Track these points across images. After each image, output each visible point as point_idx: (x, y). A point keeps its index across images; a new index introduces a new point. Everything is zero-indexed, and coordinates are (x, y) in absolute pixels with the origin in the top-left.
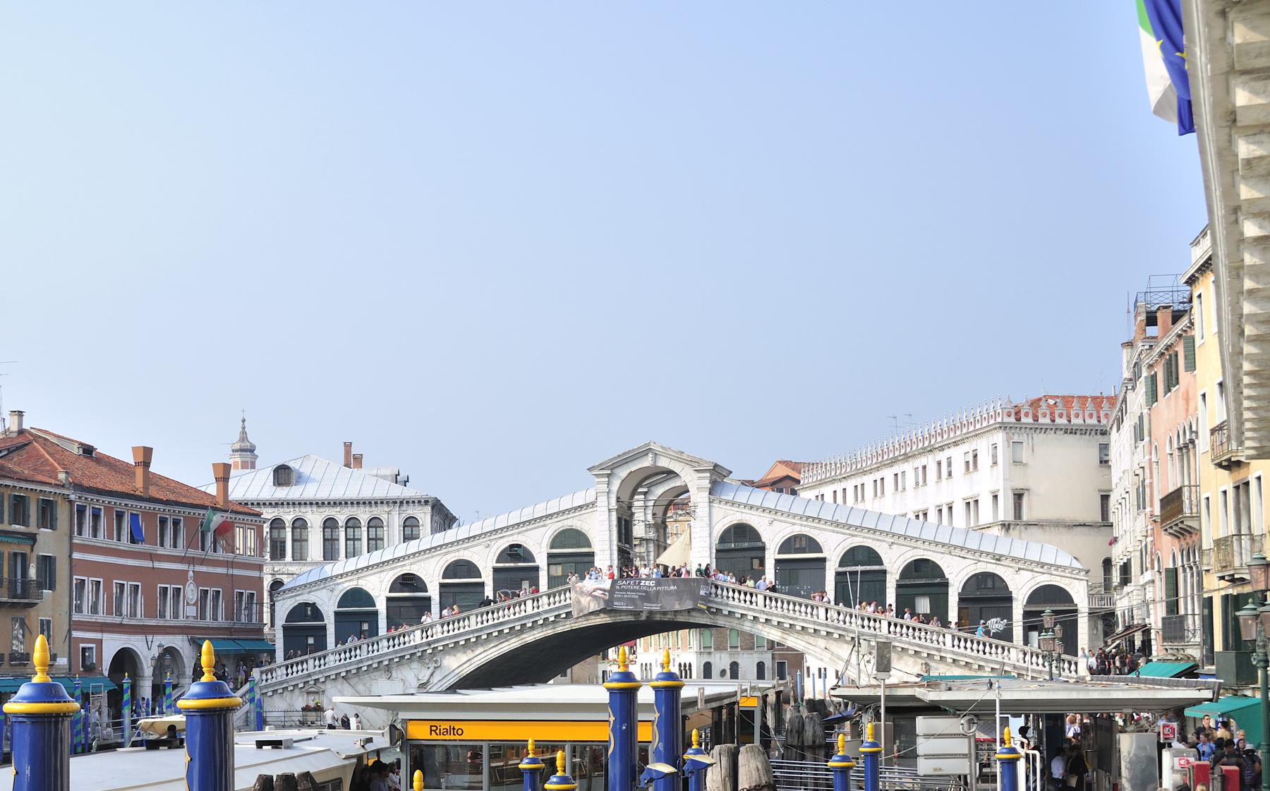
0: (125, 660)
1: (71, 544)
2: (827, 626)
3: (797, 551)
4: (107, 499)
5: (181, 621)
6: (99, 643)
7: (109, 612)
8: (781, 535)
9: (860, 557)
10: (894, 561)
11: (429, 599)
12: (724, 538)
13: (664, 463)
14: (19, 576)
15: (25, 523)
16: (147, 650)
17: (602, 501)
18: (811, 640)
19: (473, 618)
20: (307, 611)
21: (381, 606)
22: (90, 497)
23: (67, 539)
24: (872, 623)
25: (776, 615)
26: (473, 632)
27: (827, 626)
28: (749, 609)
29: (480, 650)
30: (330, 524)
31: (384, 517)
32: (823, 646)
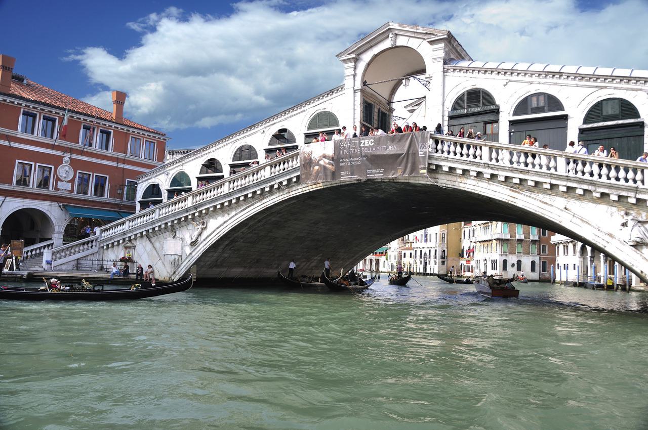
2: (568, 179)
3: (535, 111)
5: (51, 190)
8: (517, 96)
9: (610, 112)
12: (457, 104)
13: (401, 41)
17: (348, 83)
18: (547, 198)
19: (227, 184)
20: (154, 190)
24: (631, 175)
25: (503, 169)
27: (568, 179)
28: (471, 163)
29: (234, 213)
32: (562, 208)
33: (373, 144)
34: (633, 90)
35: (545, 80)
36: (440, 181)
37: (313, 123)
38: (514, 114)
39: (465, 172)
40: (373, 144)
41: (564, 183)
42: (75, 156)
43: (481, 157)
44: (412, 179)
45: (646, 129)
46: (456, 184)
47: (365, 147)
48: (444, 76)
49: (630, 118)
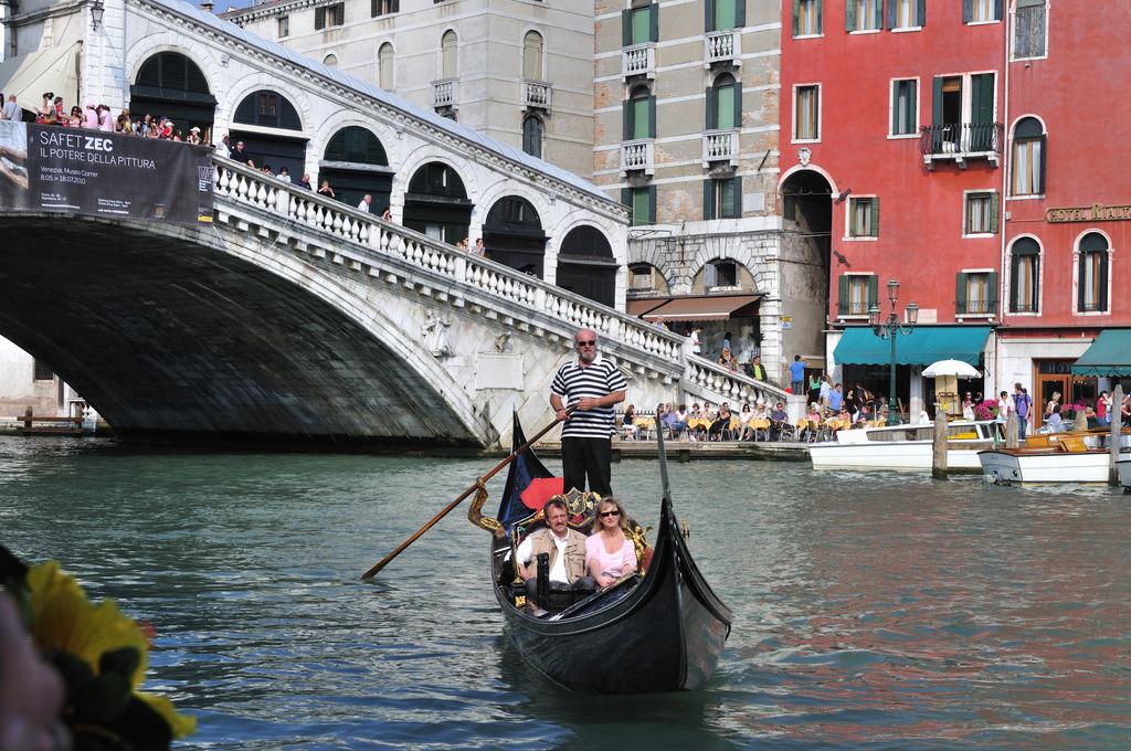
10: (404, 159)
18: (347, 283)
33: (111, 149)
34: (382, 121)
35: (280, 72)
36: (202, 236)
38: (236, 120)
39: (254, 228)
40: (111, 149)
41: (379, 265)
43: (275, 206)
44: (154, 225)
45: (395, 186)
46: (227, 245)
47: (94, 151)
48: (126, 9)
49: (379, 164)
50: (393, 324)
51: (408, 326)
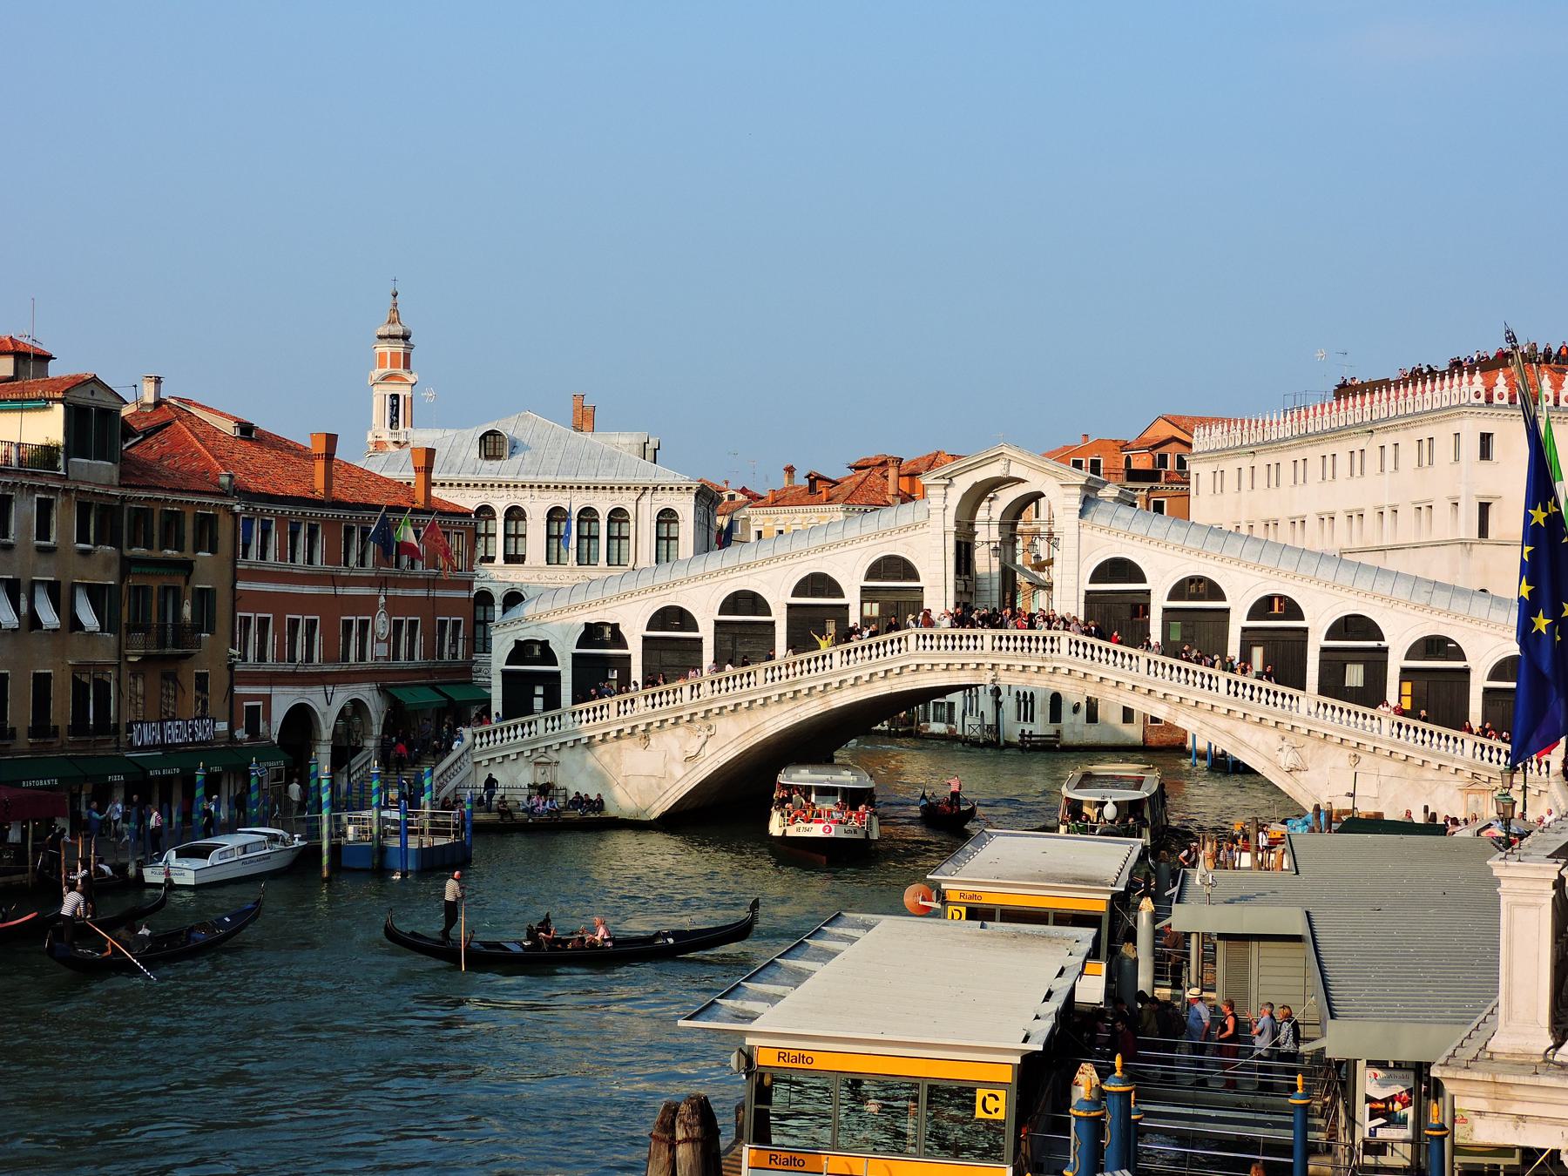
0: (301, 718)
1: (235, 570)
4: (280, 509)
6: (267, 699)
7: (280, 658)
11: (700, 640)
14: (170, 620)
15: (179, 547)
16: (327, 705)
18: (1208, 718)
21: (635, 650)
22: (259, 507)
23: (229, 564)
26: (760, 691)
30: (556, 515)
31: (630, 508)
37: (873, 573)
38: (1170, 599)
42: (391, 592)
50: (1247, 746)
51: (1262, 748)
